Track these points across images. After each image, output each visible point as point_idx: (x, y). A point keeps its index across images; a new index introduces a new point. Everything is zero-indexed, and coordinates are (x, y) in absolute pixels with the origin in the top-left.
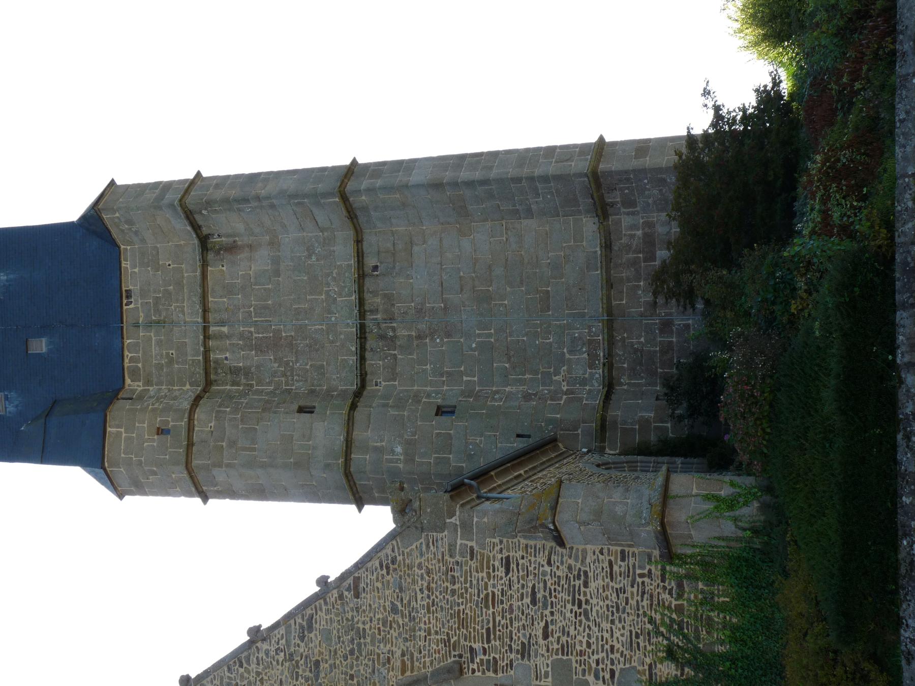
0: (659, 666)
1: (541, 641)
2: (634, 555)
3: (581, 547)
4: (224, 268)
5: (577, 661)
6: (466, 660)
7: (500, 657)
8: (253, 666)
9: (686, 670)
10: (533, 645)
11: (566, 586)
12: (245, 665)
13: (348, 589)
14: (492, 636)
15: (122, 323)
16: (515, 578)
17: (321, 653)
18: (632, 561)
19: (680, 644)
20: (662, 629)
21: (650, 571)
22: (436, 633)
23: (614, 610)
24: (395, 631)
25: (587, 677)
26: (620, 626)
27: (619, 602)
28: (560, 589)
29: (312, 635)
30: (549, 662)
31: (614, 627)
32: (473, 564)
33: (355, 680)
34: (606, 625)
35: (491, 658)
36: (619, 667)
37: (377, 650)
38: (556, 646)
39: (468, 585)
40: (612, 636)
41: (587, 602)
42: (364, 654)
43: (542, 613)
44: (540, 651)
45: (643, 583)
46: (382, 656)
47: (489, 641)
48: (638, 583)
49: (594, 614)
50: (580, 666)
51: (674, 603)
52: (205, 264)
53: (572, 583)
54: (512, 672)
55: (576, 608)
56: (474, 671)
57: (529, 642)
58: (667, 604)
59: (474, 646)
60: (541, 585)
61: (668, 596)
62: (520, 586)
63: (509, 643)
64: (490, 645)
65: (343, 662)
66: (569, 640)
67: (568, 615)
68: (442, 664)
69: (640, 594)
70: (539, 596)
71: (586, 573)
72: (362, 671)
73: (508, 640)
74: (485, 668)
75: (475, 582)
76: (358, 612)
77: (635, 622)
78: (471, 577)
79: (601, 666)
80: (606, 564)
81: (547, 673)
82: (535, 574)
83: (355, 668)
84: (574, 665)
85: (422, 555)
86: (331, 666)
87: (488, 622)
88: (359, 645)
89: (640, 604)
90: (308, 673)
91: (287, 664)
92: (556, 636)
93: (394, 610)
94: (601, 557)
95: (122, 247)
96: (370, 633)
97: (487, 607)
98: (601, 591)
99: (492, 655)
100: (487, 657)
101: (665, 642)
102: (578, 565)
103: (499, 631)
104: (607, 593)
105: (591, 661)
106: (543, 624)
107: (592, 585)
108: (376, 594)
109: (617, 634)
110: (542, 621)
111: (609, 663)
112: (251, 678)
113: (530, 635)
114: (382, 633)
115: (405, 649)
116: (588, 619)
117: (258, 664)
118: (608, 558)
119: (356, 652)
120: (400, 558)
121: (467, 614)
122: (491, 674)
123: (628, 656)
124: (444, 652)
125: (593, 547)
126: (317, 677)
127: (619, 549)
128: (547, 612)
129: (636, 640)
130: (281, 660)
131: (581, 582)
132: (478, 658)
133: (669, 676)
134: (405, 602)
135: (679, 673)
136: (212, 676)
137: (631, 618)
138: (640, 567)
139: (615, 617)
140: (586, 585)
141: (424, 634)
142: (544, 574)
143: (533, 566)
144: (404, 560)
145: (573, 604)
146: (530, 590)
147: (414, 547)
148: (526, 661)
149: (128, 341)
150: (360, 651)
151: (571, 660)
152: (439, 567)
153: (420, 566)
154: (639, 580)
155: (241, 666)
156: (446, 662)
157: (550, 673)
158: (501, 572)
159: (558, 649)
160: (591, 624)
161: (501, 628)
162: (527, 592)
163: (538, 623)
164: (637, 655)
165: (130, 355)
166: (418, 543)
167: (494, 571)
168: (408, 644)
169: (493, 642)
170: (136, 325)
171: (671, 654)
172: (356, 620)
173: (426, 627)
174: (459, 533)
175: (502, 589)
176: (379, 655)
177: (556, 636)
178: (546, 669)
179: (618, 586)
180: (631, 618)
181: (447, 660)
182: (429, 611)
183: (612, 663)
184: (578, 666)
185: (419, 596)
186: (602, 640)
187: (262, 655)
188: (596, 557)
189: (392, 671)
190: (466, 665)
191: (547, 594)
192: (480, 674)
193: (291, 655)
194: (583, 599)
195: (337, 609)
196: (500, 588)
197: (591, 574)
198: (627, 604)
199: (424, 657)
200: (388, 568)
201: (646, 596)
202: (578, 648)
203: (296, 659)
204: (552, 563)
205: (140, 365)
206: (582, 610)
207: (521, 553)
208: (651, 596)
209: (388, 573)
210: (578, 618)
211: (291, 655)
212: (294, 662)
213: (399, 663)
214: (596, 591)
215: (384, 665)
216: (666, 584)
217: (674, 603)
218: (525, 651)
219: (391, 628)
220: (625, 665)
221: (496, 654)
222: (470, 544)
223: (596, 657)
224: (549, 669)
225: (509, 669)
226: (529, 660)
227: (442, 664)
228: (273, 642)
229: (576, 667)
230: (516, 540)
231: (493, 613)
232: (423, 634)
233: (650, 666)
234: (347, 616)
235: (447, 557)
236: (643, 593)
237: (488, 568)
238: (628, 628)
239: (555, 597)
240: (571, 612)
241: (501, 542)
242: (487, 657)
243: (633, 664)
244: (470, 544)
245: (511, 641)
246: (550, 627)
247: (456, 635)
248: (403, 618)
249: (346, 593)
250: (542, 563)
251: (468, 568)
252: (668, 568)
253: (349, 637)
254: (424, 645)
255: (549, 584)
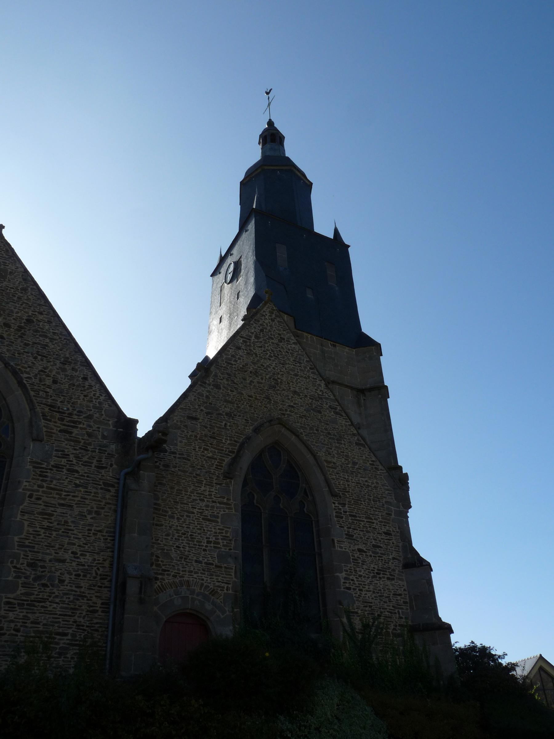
0: (358, 618)
1: (356, 547)
2: (407, 609)
3: (404, 578)
4: (350, 397)
5: (351, 567)
6: (339, 500)
7: (344, 521)
8: (312, 375)
9: (360, 636)
10: (354, 542)
11: (385, 567)
12: (311, 371)
13: (358, 440)
14: (353, 518)
15: (324, 339)
16: (383, 537)
17: (325, 416)
18: (404, 607)
19: (372, 633)
20: (376, 623)
21: (401, 618)
22: (348, 485)
23: (380, 594)
24: (344, 461)
25: (344, 573)
26: (373, 596)
27: (384, 598)
28: (383, 563)
29: (332, 413)
30: (347, 550)
31: (371, 593)
32: (384, 514)
33: (316, 432)
34: (372, 587)
35: (343, 515)
36: (353, 593)
37: (333, 448)
38: (356, 555)
39: (374, 509)
40: (367, 591)
41: (380, 578)
42: (330, 440)
43: (370, 550)
44: (352, 546)
45: (396, 613)
46: (331, 450)
47: (351, 516)
48: (395, 610)
49: (376, 582)
50: (349, 569)
51: (390, 631)
52: (352, 388)
53: (387, 570)
54: (338, 527)
55: (376, 571)
56: (334, 503)
57: (355, 540)
58: (389, 626)
59: (347, 506)
60: (383, 552)
61: (393, 627)
62: (380, 539)
63: (352, 527)
64: (349, 516)
65: (324, 427)
66: (360, 564)
67: (372, 566)
68: (334, 485)
69: (391, 611)
70: (378, 550)
71: (393, 579)
72: (321, 437)
73: (353, 527)
74: (337, 510)
75: (377, 513)
76: (349, 442)
77: (376, 606)
78: (379, 511)
79: (352, 582)
80: (400, 593)
81: (341, 547)
82: (387, 549)
83: (322, 433)
84: (349, 565)
85: (383, 485)
86: (320, 420)
87: (360, 517)
88: (333, 439)
89: (386, 610)
90: (314, 406)
91: (316, 394)
92: (360, 556)
93: (355, 463)
94: (403, 589)
95: (354, 350)
96: (341, 447)
97: (366, 518)
98: (387, 587)
99: (344, 516)
100: (343, 513)
101: (371, 623)
102: (396, 575)
103: (357, 523)
104: (387, 590)
105: (352, 576)
106: (364, 549)
107: (388, 583)
108: (360, 455)
109: (369, 594)
110: (366, 549)
111: (354, 587)
112: (306, 372)
113: (358, 541)
114: (342, 454)
115: (337, 465)
116: (373, 577)
117: (313, 379)
118: (403, 593)
119: (330, 436)
120: (378, 472)
121: (361, 505)
122: (334, 514)
123: (359, 599)
124: (340, 487)
125: (405, 585)
126: (313, 410)
127: (408, 600)
128: (371, 553)
129: (368, 606)
130: (318, 392)
131: (389, 576)
132: (341, 507)
133: (354, 624)
134: (359, 470)
135: (357, 630)
136: (302, 350)
137: (378, 604)
138: (402, 612)
139: (376, 594)
140: (388, 579)
141: (346, 478)
142: (388, 555)
143: (391, 549)
144: (378, 475)
145: (378, 570)
146: (379, 544)
147: (385, 482)
148: (345, 536)
149: (315, 338)
150: (330, 438)
151: (351, 564)
152: (379, 494)
153: (377, 483)
154: (396, 611)
155: (310, 368)
156: (335, 488)
157: (342, 550)
158: (383, 529)
159: (354, 556)
160: (370, 579)
161: (358, 524)
162: (377, 543)
163: (365, 547)
164: (361, 605)
165: (309, 337)
166: (387, 485)
167: (384, 525)
168: (340, 467)
169: (350, 518)
170: (322, 345)
171: (366, 626)
172: (345, 440)
173: (350, 480)
174: (396, 509)
175: (376, 529)
176: (331, 449)
177: (360, 556)
178: (344, 547)
179: (391, 598)
180: (378, 604)
181: (336, 488)
182: (357, 483)
183: (354, 589)
184: (349, 568)
185: (363, 479)
186: (364, 585)
187: (318, 382)
188: (402, 586)
189: (325, 455)
190: (336, 499)
191: (379, 555)
192: (334, 507)
193: (321, 399)
194: (381, 576)
195: (348, 431)
196: (377, 527)
197: (393, 582)
198: (384, 602)
199: (335, 475)
200: (373, 465)
201: (390, 614)
202: (358, 569)
203: (320, 400)
204: (394, 560)
205: (305, 340)
206: (375, 574)
207: (395, 543)
208: (391, 618)
209: (370, 464)
210: (372, 572)
211: (321, 399)
212: (318, 399)
213: (329, 460)
214: (386, 584)
215: (327, 451)
216: (398, 627)
217: (390, 631)
218: (349, 536)
219: (345, 459)
220: (355, 597)
221: (345, 518)
222: (393, 514)
223: (355, 579)
224: (344, 550)
225: (339, 525)
226: (346, 538)
227: (334, 485)
228: (326, 390)
229: (348, 566)
230: (400, 541)
231: (364, 521)
232: (347, 477)
233: (357, 613)
234: (346, 435)
235: (384, 500)
236: (391, 613)
237: (385, 522)
238: (373, 601)
239: (379, 559)
240: (374, 568)
241: (398, 532)
242: (343, 513)
243: (356, 602)
244: (393, 514)
245: (353, 529)
246: (364, 554)
247: (349, 496)
248: (352, 467)
249: (356, 438)
250: (393, 554)
251: (382, 511)
252: (406, 629)
253: (336, 434)
254: (341, 477)
255: (384, 557)
